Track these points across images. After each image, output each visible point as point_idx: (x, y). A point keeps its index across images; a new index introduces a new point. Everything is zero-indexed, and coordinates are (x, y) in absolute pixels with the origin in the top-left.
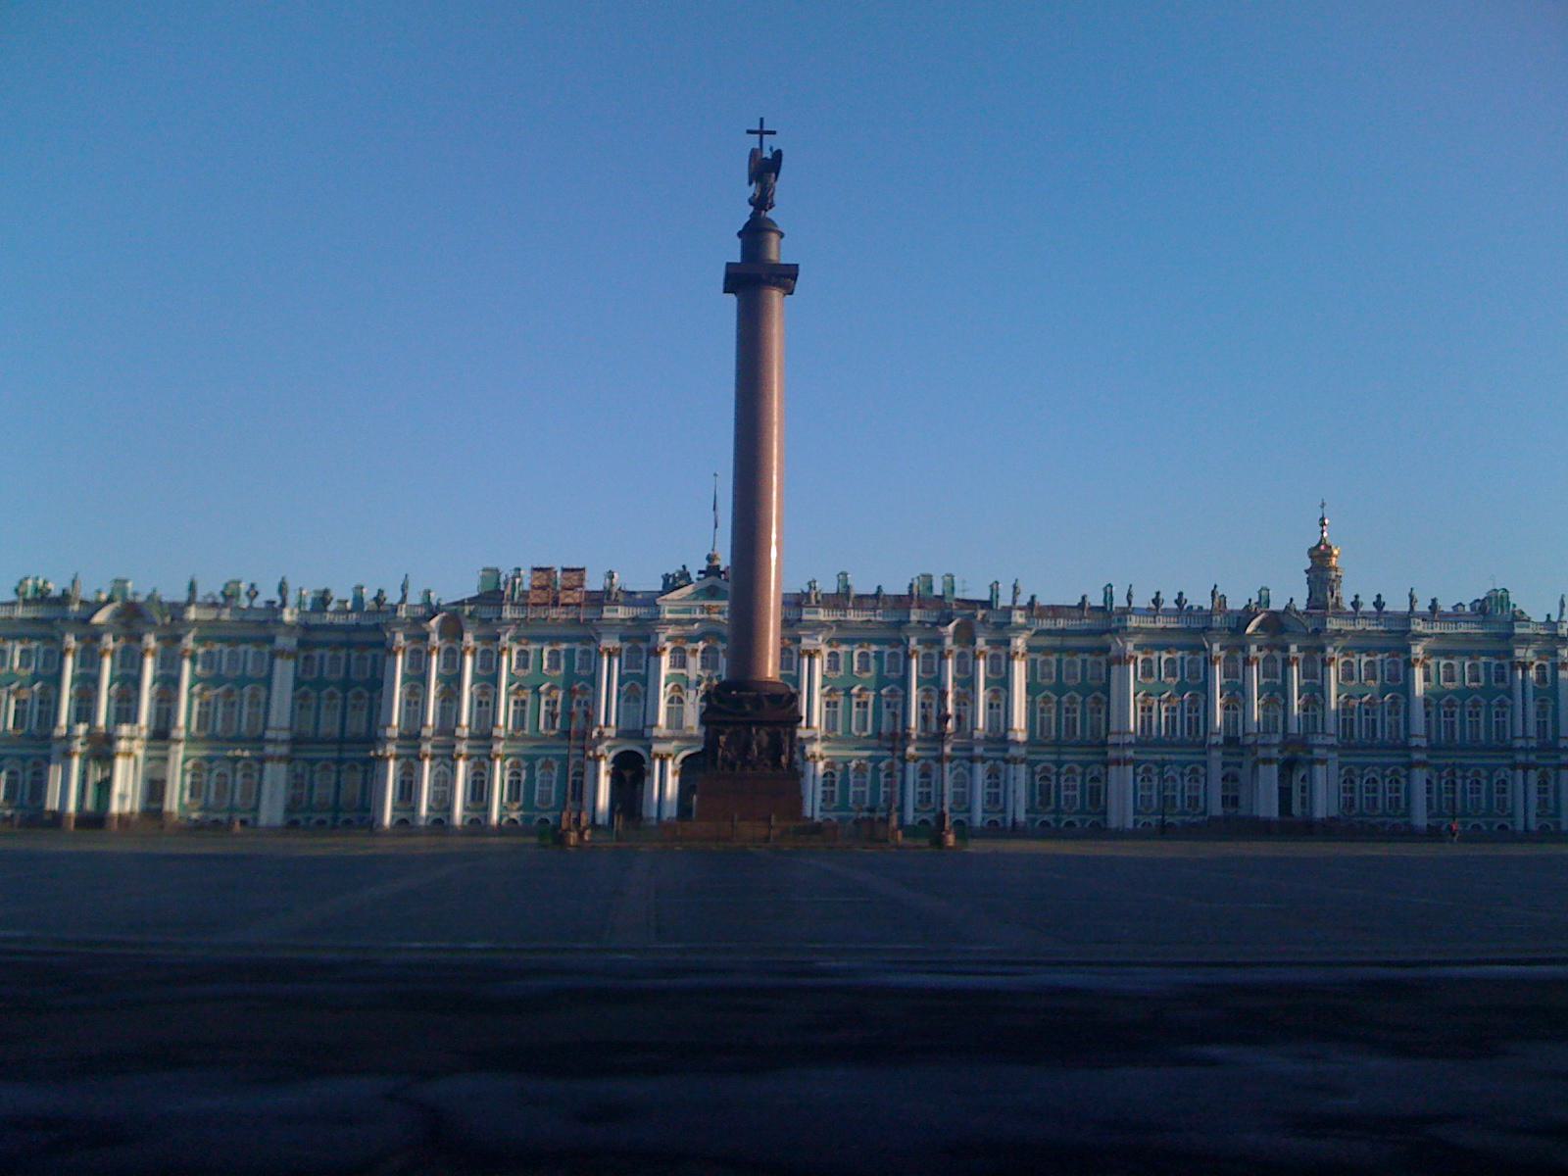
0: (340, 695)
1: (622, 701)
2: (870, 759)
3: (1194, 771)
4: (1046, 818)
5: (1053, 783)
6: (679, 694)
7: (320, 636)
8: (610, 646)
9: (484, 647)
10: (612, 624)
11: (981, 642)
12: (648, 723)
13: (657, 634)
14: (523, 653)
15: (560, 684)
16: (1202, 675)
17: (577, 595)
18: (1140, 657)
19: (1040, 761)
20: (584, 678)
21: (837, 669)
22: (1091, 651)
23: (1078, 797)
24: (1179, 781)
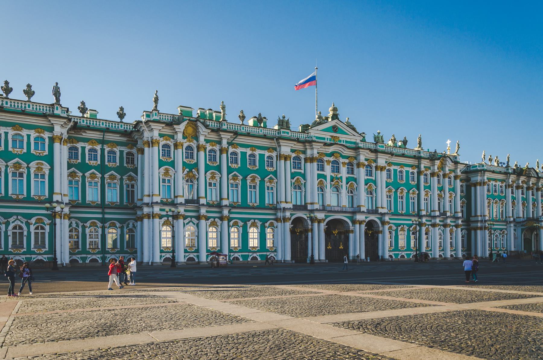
0: (99, 175)
20: (271, 173)
21: (390, 178)
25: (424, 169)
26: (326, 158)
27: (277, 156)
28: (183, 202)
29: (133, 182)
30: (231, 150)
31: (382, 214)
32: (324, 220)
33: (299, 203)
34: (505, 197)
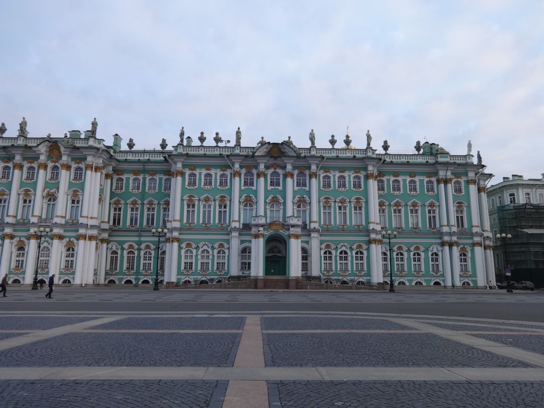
3: (221, 245)
4: (129, 278)
5: (136, 255)
11: (64, 158)
18: (188, 172)
19: (125, 242)
34: (230, 191)
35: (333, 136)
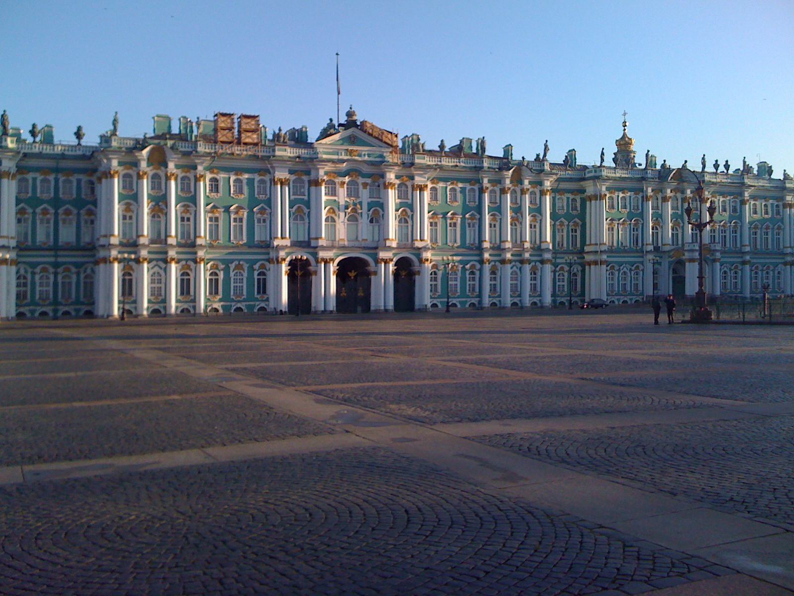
0: (52, 211)
1: (292, 219)
2: (460, 262)
3: (637, 267)
6: (333, 215)
7: (33, 163)
8: (282, 177)
9: (184, 174)
10: (282, 160)
12: (313, 235)
13: (318, 169)
14: (214, 180)
15: (245, 205)
16: (640, 208)
17: (255, 136)
20: (261, 202)
21: (436, 199)
22: (571, 192)
23: (566, 287)
24: (629, 274)
25: (489, 185)
26: (338, 180)
27: (270, 180)
28: (147, 243)
29: (93, 217)
30: (209, 176)
31: (419, 249)
32: (333, 260)
33: (301, 239)
35: (717, 161)
